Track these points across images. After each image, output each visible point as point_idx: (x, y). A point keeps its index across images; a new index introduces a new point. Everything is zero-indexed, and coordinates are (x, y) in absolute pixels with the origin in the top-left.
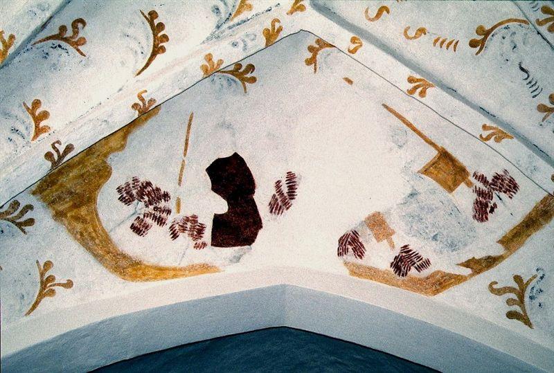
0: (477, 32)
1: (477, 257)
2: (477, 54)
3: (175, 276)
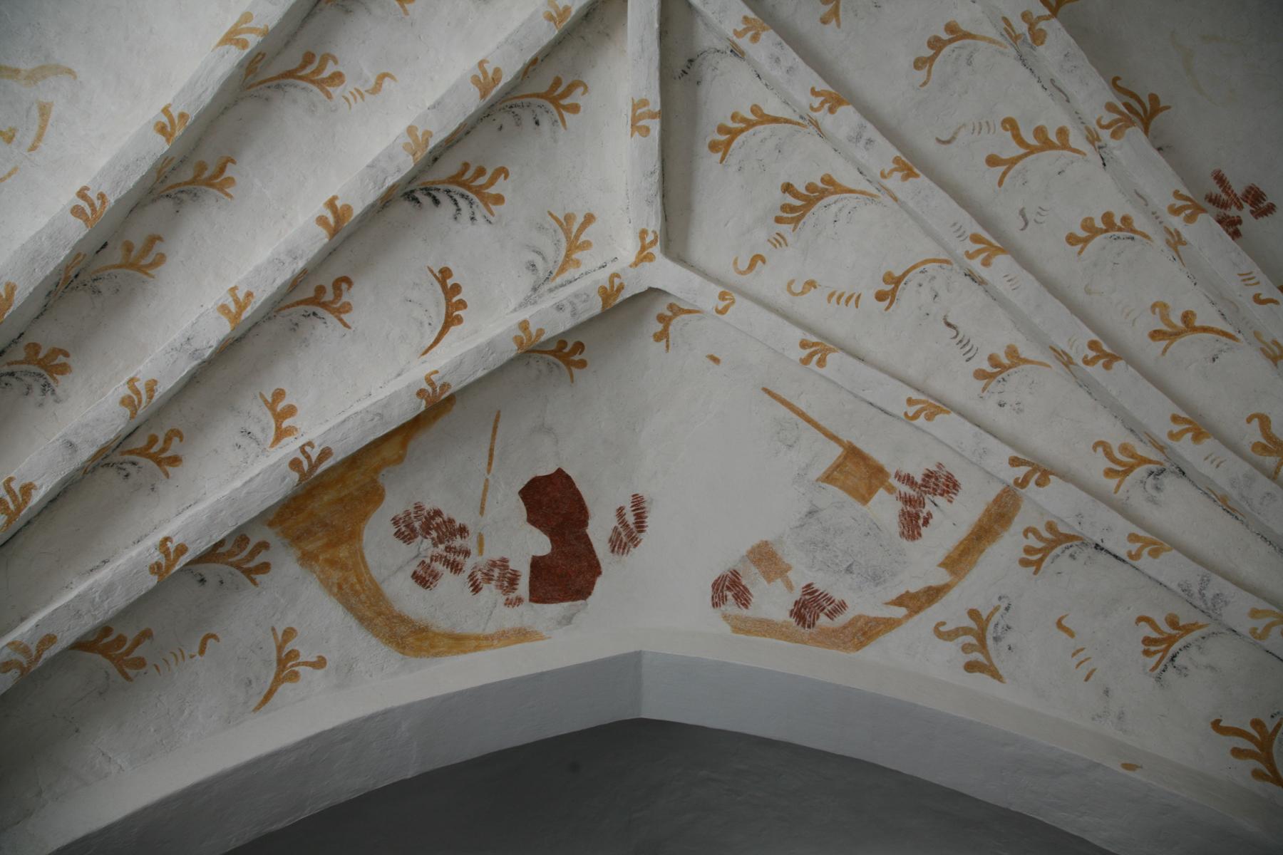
0: (884, 280)
1: (913, 590)
2: (888, 308)
3: (477, 648)
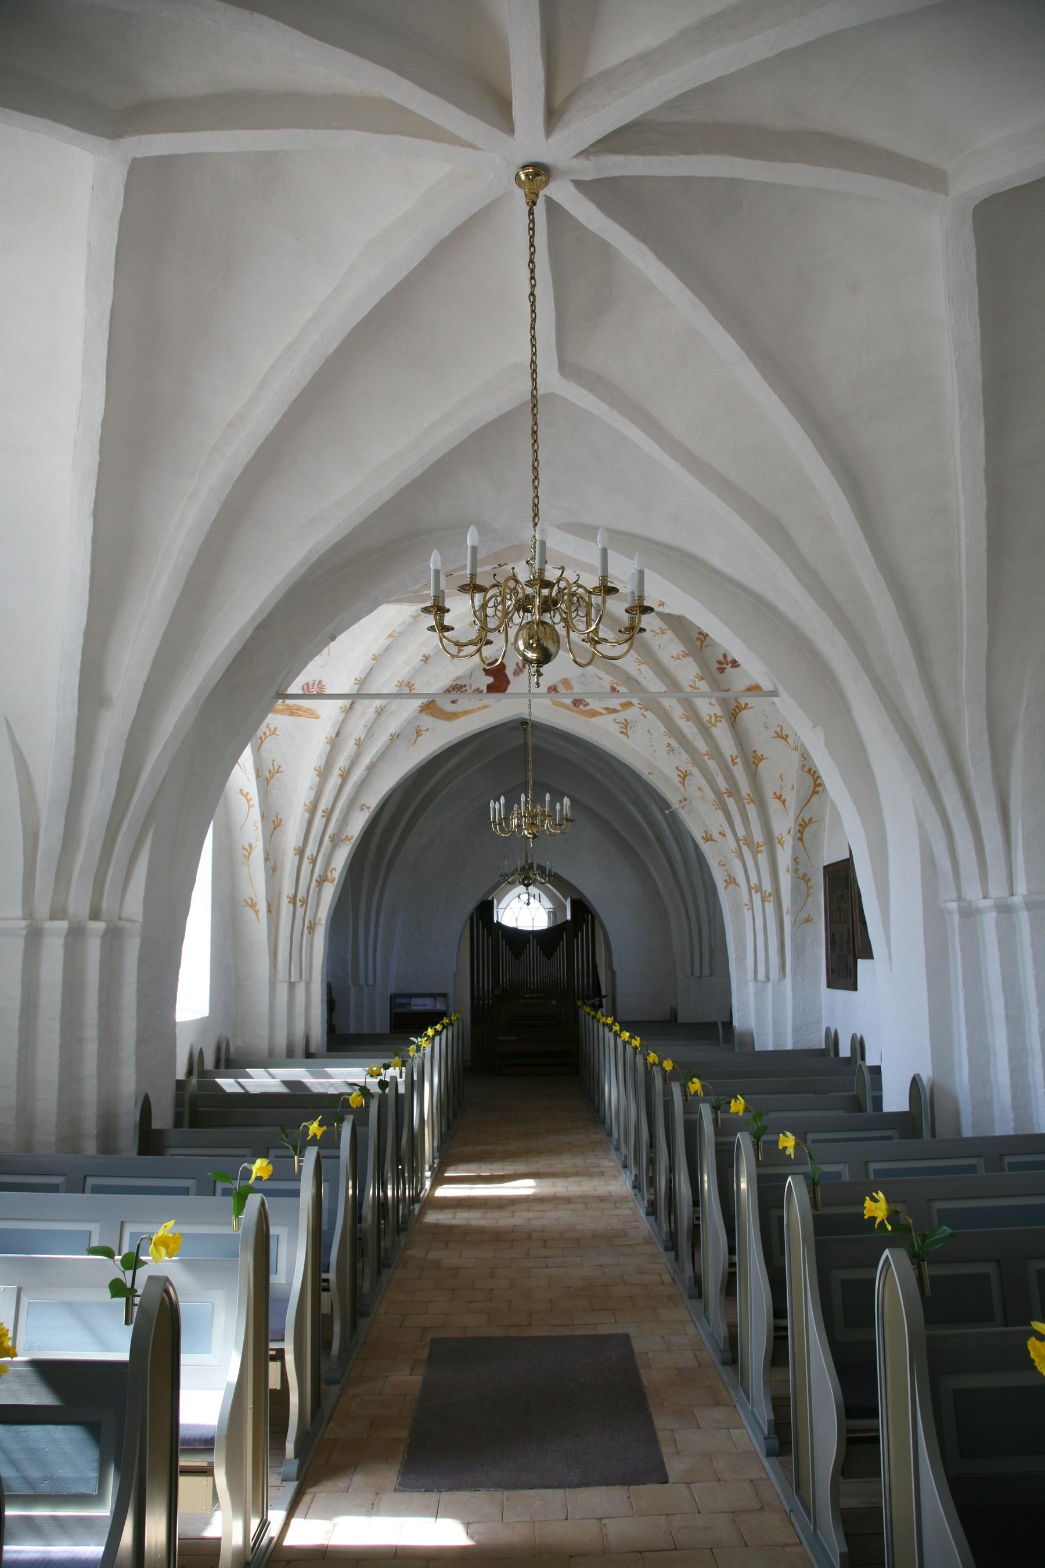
1: (610, 707)
3: (472, 713)
